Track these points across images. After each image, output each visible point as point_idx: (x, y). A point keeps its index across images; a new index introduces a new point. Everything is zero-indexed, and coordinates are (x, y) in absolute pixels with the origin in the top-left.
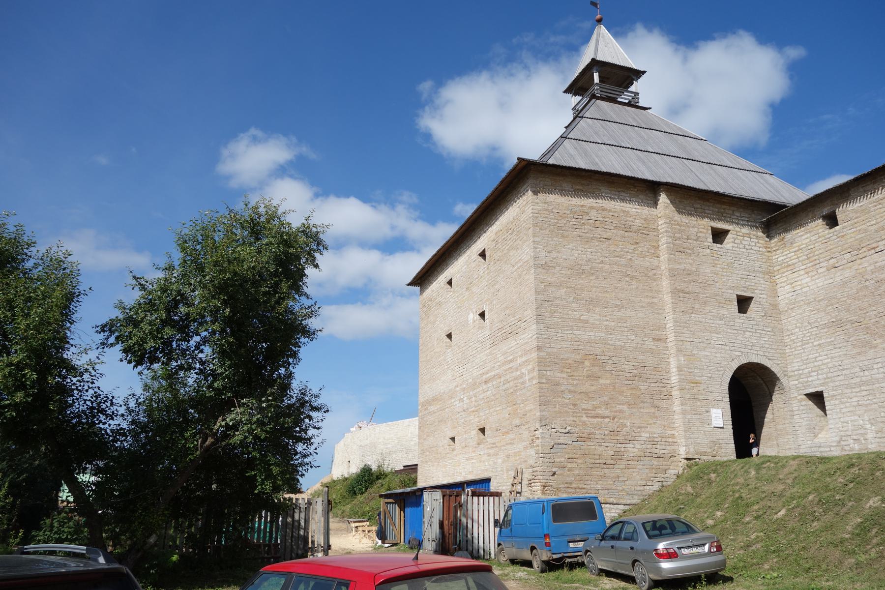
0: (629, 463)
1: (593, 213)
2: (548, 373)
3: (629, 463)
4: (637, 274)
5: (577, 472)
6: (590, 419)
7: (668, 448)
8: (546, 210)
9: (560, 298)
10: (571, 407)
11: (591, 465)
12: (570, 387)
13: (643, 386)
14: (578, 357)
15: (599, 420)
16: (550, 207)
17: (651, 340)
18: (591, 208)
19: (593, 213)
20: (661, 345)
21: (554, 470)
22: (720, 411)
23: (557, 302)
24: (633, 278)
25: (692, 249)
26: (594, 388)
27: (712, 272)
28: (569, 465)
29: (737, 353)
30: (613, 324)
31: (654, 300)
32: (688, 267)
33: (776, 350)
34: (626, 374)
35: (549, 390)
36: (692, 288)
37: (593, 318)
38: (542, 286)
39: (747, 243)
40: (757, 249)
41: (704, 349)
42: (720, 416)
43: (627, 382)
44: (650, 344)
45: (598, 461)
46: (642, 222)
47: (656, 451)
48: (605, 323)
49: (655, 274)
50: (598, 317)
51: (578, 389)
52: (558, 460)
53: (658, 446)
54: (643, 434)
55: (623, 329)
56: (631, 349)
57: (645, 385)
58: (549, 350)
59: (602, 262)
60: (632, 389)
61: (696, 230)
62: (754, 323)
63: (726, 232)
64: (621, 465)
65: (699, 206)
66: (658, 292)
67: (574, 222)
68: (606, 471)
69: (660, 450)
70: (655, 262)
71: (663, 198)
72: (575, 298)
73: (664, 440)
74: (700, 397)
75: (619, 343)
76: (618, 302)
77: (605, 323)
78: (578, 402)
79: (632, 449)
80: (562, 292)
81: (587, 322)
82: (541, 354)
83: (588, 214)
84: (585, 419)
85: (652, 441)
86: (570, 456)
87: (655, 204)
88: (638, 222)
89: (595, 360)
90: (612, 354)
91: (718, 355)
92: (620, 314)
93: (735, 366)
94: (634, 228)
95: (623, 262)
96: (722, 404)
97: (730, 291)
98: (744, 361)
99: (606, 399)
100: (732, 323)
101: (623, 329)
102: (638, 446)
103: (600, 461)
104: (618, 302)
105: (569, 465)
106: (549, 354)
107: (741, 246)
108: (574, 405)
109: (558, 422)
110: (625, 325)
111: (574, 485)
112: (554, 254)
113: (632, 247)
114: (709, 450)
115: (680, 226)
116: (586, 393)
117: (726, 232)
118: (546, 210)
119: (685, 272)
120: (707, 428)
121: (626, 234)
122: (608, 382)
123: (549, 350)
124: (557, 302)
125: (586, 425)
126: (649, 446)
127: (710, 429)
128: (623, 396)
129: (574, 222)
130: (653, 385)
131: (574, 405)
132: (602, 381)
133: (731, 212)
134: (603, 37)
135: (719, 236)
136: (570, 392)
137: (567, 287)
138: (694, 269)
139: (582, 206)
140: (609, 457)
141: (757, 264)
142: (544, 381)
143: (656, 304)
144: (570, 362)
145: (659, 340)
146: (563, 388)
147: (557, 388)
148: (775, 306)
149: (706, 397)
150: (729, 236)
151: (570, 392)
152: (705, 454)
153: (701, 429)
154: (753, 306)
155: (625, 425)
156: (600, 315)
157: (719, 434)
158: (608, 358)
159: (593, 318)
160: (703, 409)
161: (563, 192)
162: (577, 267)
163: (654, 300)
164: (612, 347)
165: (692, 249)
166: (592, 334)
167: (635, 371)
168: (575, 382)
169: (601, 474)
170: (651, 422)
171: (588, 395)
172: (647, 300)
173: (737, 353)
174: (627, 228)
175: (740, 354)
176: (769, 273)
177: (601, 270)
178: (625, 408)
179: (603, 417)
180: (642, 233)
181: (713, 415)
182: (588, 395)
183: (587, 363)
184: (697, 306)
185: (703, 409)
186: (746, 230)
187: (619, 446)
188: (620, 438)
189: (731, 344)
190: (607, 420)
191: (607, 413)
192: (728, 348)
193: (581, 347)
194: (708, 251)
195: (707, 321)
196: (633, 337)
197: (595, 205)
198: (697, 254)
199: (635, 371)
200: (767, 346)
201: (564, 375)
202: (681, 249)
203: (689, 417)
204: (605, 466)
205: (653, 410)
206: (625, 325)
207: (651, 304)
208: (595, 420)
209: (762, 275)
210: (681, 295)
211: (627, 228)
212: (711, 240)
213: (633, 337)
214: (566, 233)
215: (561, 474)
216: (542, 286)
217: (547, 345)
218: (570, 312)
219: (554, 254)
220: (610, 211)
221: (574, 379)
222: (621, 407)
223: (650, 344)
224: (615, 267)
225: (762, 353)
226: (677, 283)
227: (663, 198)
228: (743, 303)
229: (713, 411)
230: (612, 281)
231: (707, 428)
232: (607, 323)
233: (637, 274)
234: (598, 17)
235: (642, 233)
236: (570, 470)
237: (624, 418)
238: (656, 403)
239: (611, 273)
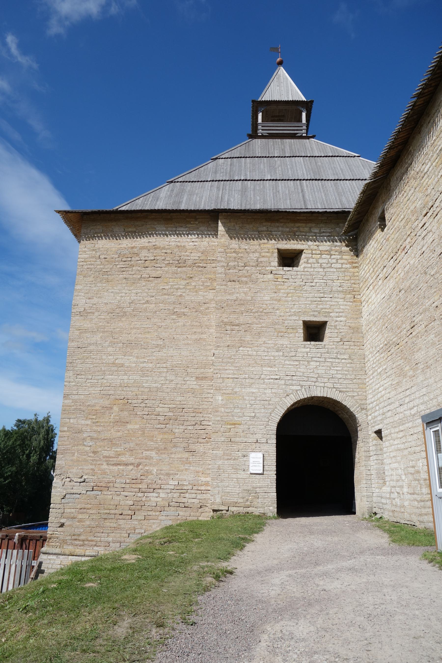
0: (150, 513)
2: (72, 421)
3: (150, 513)
4: (186, 310)
5: (88, 523)
6: (111, 467)
7: (199, 497)
8: (92, 257)
9: (96, 344)
10: (91, 455)
11: (105, 516)
12: (92, 434)
14: (107, 403)
15: (121, 467)
16: (98, 254)
17: (194, 379)
18: (143, 248)
19: (144, 253)
20: (205, 383)
21: (63, 521)
22: (260, 455)
23: (92, 347)
25: (250, 276)
26: (119, 434)
27: (272, 299)
28: (80, 516)
29: (295, 388)
30: (151, 365)
31: (204, 336)
32: (242, 296)
33: (352, 380)
34: (159, 417)
36: (242, 320)
39: (324, 261)
40: (339, 266)
41: (250, 386)
42: (260, 462)
43: (159, 426)
44: (192, 383)
45: (113, 512)
46: (199, 254)
47: (184, 500)
48: (142, 365)
49: (208, 308)
50: (135, 359)
51: (102, 436)
52: (69, 510)
53: (187, 495)
54: (171, 482)
55: (162, 370)
56: (168, 390)
58: (76, 397)
59: (147, 302)
60: (165, 433)
61: (257, 255)
63: (299, 253)
64: (140, 516)
65: (265, 228)
66: (208, 327)
67: (121, 265)
68: (121, 522)
69: (190, 498)
70: (210, 295)
71: (221, 228)
72: (111, 342)
73: (195, 488)
74: (238, 439)
75: (154, 385)
76: (160, 342)
77: (142, 365)
78: (99, 449)
80: (97, 337)
81: (122, 365)
82: (66, 401)
83: (137, 255)
84: (105, 466)
85: (181, 490)
86: (83, 506)
87: (215, 234)
88: (195, 256)
89: (124, 404)
90: (145, 397)
91: (268, 391)
92: (160, 354)
93: (289, 402)
94: (189, 263)
95: (172, 299)
96: (265, 447)
97: (294, 318)
98: (303, 395)
99: (132, 445)
100: (293, 354)
101: (162, 370)
102: (162, 495)
103: (116, 512)
104: (160, 342)
105: (80, 516)
106: (75, 401)
107: (316, 265)
108: (94, 452)
109: (74, 471)
110: (164, 365)
111: (82, 537)
112: (95, 300)
113: (184, 282)
114: (241, 500)
115: (237, 253)
116: (111, 440)
117: (299, 253)
118: (92, 257)
119: (236, 303)
120: (242, 475)
121: (179, 269)
122: (137, 427)
123: (76, 397)
124: (92, 347)
125: (105, 473)
126: (176, 495)
127: (245, 476)
128: (152, 441)
129: (121, 265)
130: (190, 428)
131: (94, 452)
132: (129, 426)
133: (307, 229)
134: (278, 79)
136: (92, 439)
137: (103, 332)
138: (249, 298)
139: (133, 248)
140: (127, 508)
141: (337, 283)
142: (66, 429)
143: (204, 340)
144: (97, 408)
146: (85, 435)
147: (78, 435)
148: (356, 330)
149: (245, 440)
150: (303, 256)
151: (92, 439)
152: (235, 504)
153: (234, 476)
154: (328, 332)
156: (137, 357)
157: (258, 482)
158: (140, 401)
160: (240, 454)
161: (115, 236)
162: (118, 311)
163: (204, 336)
164: (147, 390)
165: (250, 276)
166: (126, 377)
168: (99, 429)
169: (115, 525)
170: (182, 467)
171: (111, 442)
172: (194, 337)
173: (295, 388)
174: (181, 263)
175: (299, 388)
176: (354, 294)
177: (146, 310)
178: (153, 454)
179: (126, 465)
180: (199, 267)
181: (251, 460)
183: (116, 408)
184: (248, 338)
185: (240, 454)
186: (326, 246)
187: (140, 495)
188: (143, 486)
189: (288, 378)
190: (131, 467)
191: (131, 460)
192: (283, 382)
193: (110, 392)
194: (271, 276)
195: (259, 353)
196: (173, 378)
197: (147, 245)
198: (255, 282)
199: (171, 414)
200: (340, 376)
201: (89, 422)
202: (235, 278)
203: (220, 462)
204: (121, 517)
205: (186, 455)
206: (164, 365)
208: (116, 468)
209: (341, 296)
210: (228, 328)
211: (181, 263)
212: (276, 264)
213: (173, 378)
214: (110, 277)
215: (69, 526)
217: (75, 392)
218: (104, 357)
219: (95, 300)
220: (164, 248)
221: (100, 426)
222: (148, 453)
223: (192, 383)
224: (162, 306)
225: (330, 385)
226: (225, 315)
227: (221, 228)
229: (252, 455)
230: (156, 320)
231: (242, 475)
232: (145, 365)
233: (186, 310)
234: (278, 60)
235: (199, 267)
236: (80, 521)
237: (151, 464)
238: (192, 447)
239: (156, 312)
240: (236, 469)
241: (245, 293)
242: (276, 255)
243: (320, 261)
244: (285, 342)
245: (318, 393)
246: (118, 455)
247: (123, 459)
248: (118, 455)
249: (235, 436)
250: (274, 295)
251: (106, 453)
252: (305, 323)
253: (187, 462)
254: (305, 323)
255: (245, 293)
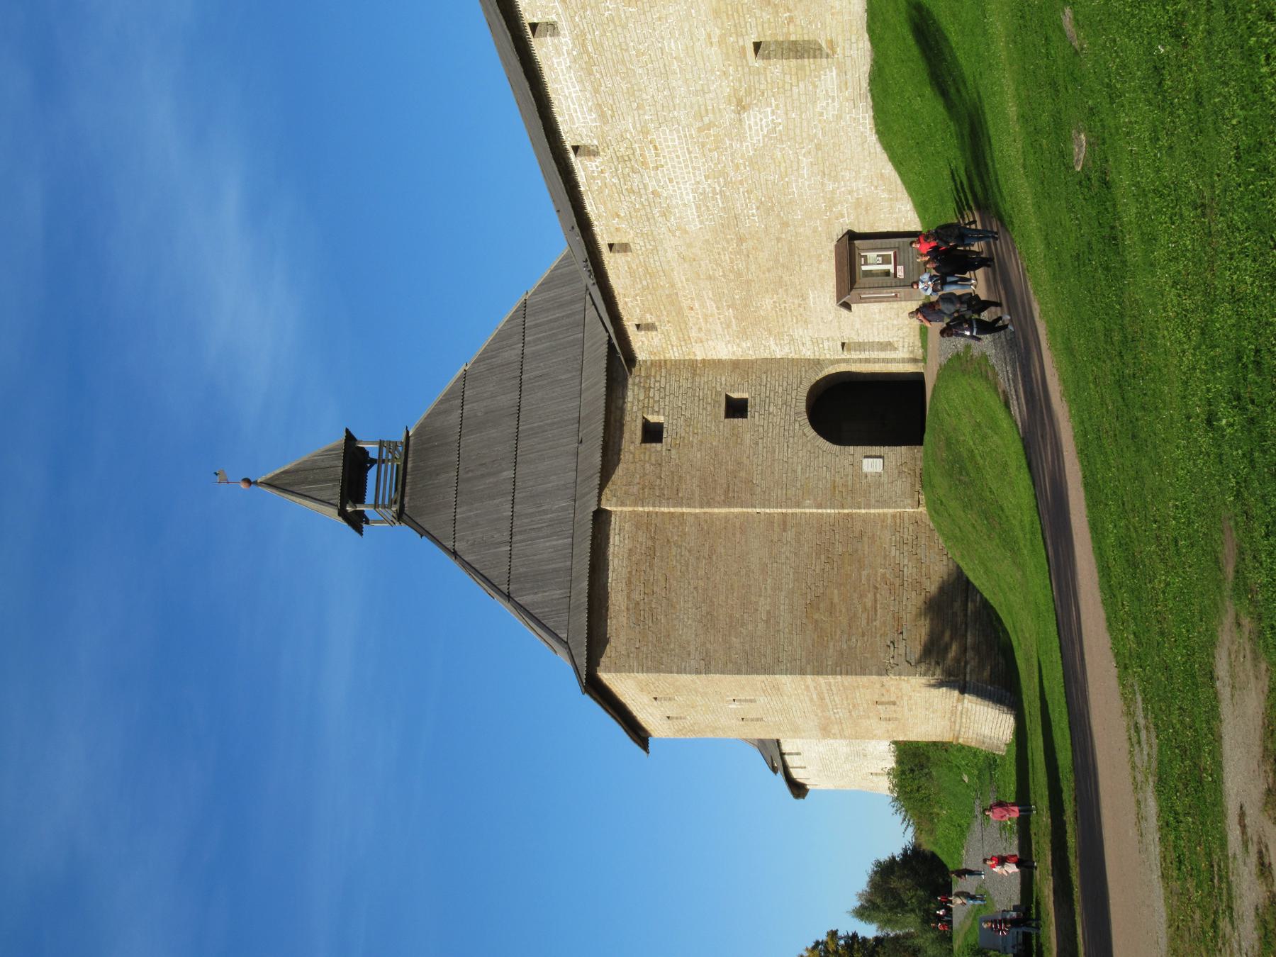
1: (636, 596)
13: (840, 549)
14: (810, 627)
22: (865, 461)
24: (713, 550)
27: (700, 450)
31: (738, 525)
35: (849, 664)
37: (764, 604)
38: (730, 666)
40: (663, 380)
41: (795, 471)
42: (873, 463)
44: (790, 535)
48: (769, 591)
54: (893, 553)
57: (839, 547)
61: (647, 465)
62: (758, 400)
69: (908, 535)
76: (743, 572)
79: (909, 570)
81: (768, 612)
84: (877, 623)
88: (642, 537)
91: (800, 454)
93: (811, 433)
94: (650, 543)
95: (692, 561)
98: (804, 418)
99: (855, 596)
100: (761, 429)
112: (692, 648)
113: (674, 551)
116: (850, 619)
120: (885, 479)
124: (747, 647)
132: (836, 600)
135: (652, 433)
145: (785, 523)
146: (845, 647)
152: (913, 486)
155: (883, 576)
159: (764, 604)
163: (738, 525)
167: (823, 557)
168: (839, 632)
171: (853, 619)
172: (738, 535)
173: (797, 426)
174: (651, 552)
177: (705, 590)
178: (864, 573)
182: (853, 619)
183: (816, 616)
188: (897, 582)
191: (870, 595)
194: (673, 452)
199: (823, 557)
201: (831, 644)
205: (865, 539)
207: (743, 532)
208: (879, 611)
209: (697, 379)
212: (658, 446)
216: (730, 666)
219: (692, 648)
223: (790, 535)
225: (794, 394)
226: (717, 498)
228: (736, 409)
231: (885, 479)
240: (879, 485)
241: (693, 477)
242: (648, 445)
243: (657, 398)
244: (748, 438)
245: (802, 406)
246: (865, 609)
247: (869, 604)
248: (865, 609)
249: (846, 486)
250: (695, 449)
251: (864, 622)
252: (727, 416)
253: (872, 538)
254: (727, 416)
255: (693, 477)
